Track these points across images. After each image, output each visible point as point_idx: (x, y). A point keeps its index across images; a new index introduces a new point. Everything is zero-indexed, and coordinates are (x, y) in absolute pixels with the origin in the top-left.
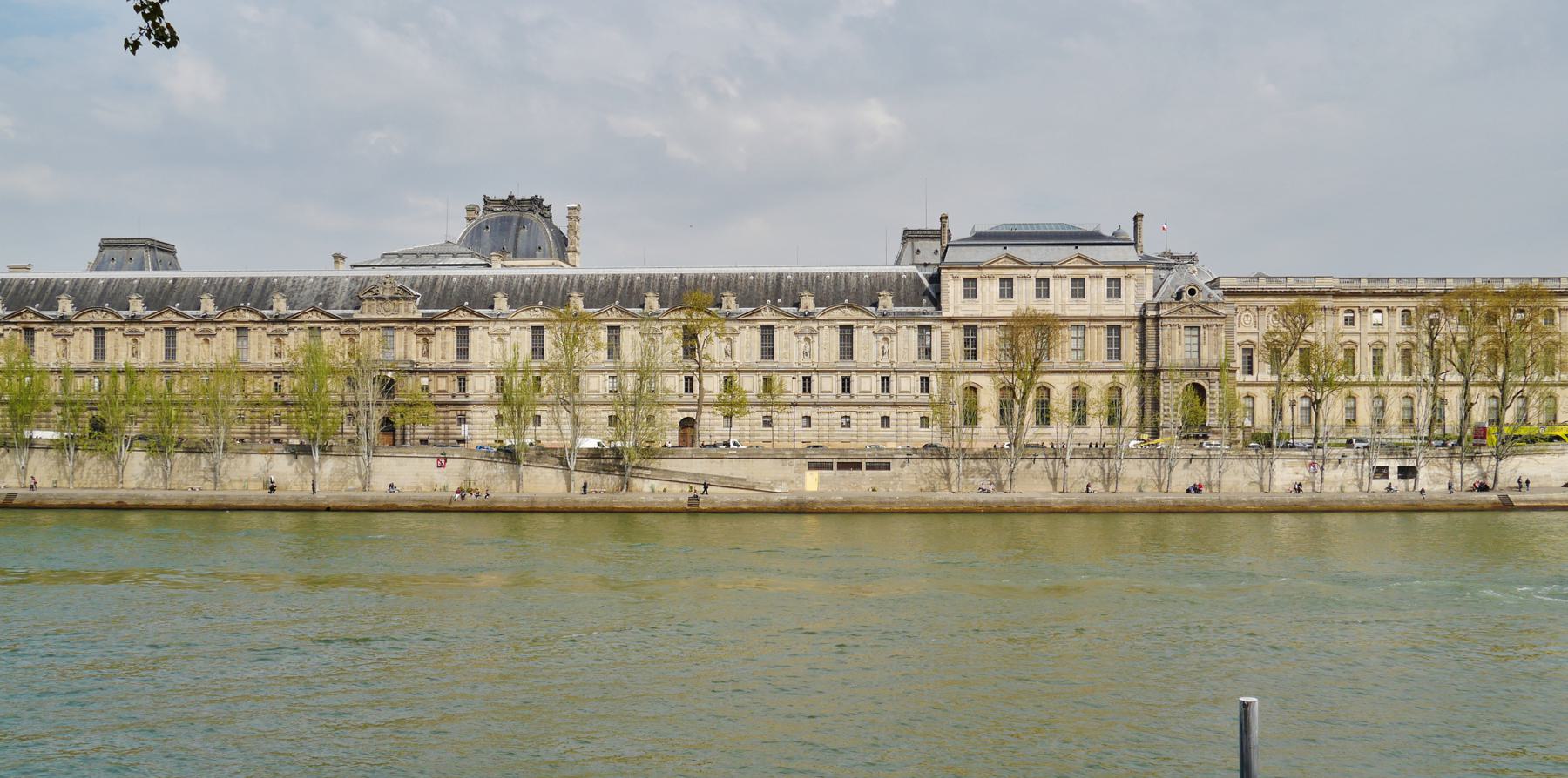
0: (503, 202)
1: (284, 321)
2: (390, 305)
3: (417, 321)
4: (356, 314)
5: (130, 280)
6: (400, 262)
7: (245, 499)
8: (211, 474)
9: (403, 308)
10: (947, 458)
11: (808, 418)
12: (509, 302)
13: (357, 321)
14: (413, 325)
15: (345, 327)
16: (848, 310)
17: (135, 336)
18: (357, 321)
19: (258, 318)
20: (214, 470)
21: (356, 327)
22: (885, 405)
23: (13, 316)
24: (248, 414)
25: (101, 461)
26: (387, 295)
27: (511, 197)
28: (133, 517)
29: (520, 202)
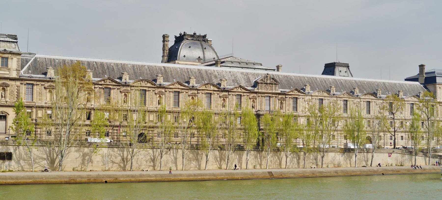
0: (191, 36)
1: (228, 91)
2: (268, 87)
3: (279, 94)
4: (256, 90)
5: (143, 66)
8: (315, 161)
9: (274, 88)
11: (402, 137)
13: (256, 93)
14: (277, 96)
15: (252, 95)
16: (413, 98)
17: (160, 95)
18: (256, 93)
19: (216, 89)
20: (315, 160)
21: (255, 95)
22: (402, 132)
23: (101, 81)
24: (111, 131)
25: (272, 156)
26: (269, 82)
27: (195, 34)
28: (210, 184)
29: (199, 36)
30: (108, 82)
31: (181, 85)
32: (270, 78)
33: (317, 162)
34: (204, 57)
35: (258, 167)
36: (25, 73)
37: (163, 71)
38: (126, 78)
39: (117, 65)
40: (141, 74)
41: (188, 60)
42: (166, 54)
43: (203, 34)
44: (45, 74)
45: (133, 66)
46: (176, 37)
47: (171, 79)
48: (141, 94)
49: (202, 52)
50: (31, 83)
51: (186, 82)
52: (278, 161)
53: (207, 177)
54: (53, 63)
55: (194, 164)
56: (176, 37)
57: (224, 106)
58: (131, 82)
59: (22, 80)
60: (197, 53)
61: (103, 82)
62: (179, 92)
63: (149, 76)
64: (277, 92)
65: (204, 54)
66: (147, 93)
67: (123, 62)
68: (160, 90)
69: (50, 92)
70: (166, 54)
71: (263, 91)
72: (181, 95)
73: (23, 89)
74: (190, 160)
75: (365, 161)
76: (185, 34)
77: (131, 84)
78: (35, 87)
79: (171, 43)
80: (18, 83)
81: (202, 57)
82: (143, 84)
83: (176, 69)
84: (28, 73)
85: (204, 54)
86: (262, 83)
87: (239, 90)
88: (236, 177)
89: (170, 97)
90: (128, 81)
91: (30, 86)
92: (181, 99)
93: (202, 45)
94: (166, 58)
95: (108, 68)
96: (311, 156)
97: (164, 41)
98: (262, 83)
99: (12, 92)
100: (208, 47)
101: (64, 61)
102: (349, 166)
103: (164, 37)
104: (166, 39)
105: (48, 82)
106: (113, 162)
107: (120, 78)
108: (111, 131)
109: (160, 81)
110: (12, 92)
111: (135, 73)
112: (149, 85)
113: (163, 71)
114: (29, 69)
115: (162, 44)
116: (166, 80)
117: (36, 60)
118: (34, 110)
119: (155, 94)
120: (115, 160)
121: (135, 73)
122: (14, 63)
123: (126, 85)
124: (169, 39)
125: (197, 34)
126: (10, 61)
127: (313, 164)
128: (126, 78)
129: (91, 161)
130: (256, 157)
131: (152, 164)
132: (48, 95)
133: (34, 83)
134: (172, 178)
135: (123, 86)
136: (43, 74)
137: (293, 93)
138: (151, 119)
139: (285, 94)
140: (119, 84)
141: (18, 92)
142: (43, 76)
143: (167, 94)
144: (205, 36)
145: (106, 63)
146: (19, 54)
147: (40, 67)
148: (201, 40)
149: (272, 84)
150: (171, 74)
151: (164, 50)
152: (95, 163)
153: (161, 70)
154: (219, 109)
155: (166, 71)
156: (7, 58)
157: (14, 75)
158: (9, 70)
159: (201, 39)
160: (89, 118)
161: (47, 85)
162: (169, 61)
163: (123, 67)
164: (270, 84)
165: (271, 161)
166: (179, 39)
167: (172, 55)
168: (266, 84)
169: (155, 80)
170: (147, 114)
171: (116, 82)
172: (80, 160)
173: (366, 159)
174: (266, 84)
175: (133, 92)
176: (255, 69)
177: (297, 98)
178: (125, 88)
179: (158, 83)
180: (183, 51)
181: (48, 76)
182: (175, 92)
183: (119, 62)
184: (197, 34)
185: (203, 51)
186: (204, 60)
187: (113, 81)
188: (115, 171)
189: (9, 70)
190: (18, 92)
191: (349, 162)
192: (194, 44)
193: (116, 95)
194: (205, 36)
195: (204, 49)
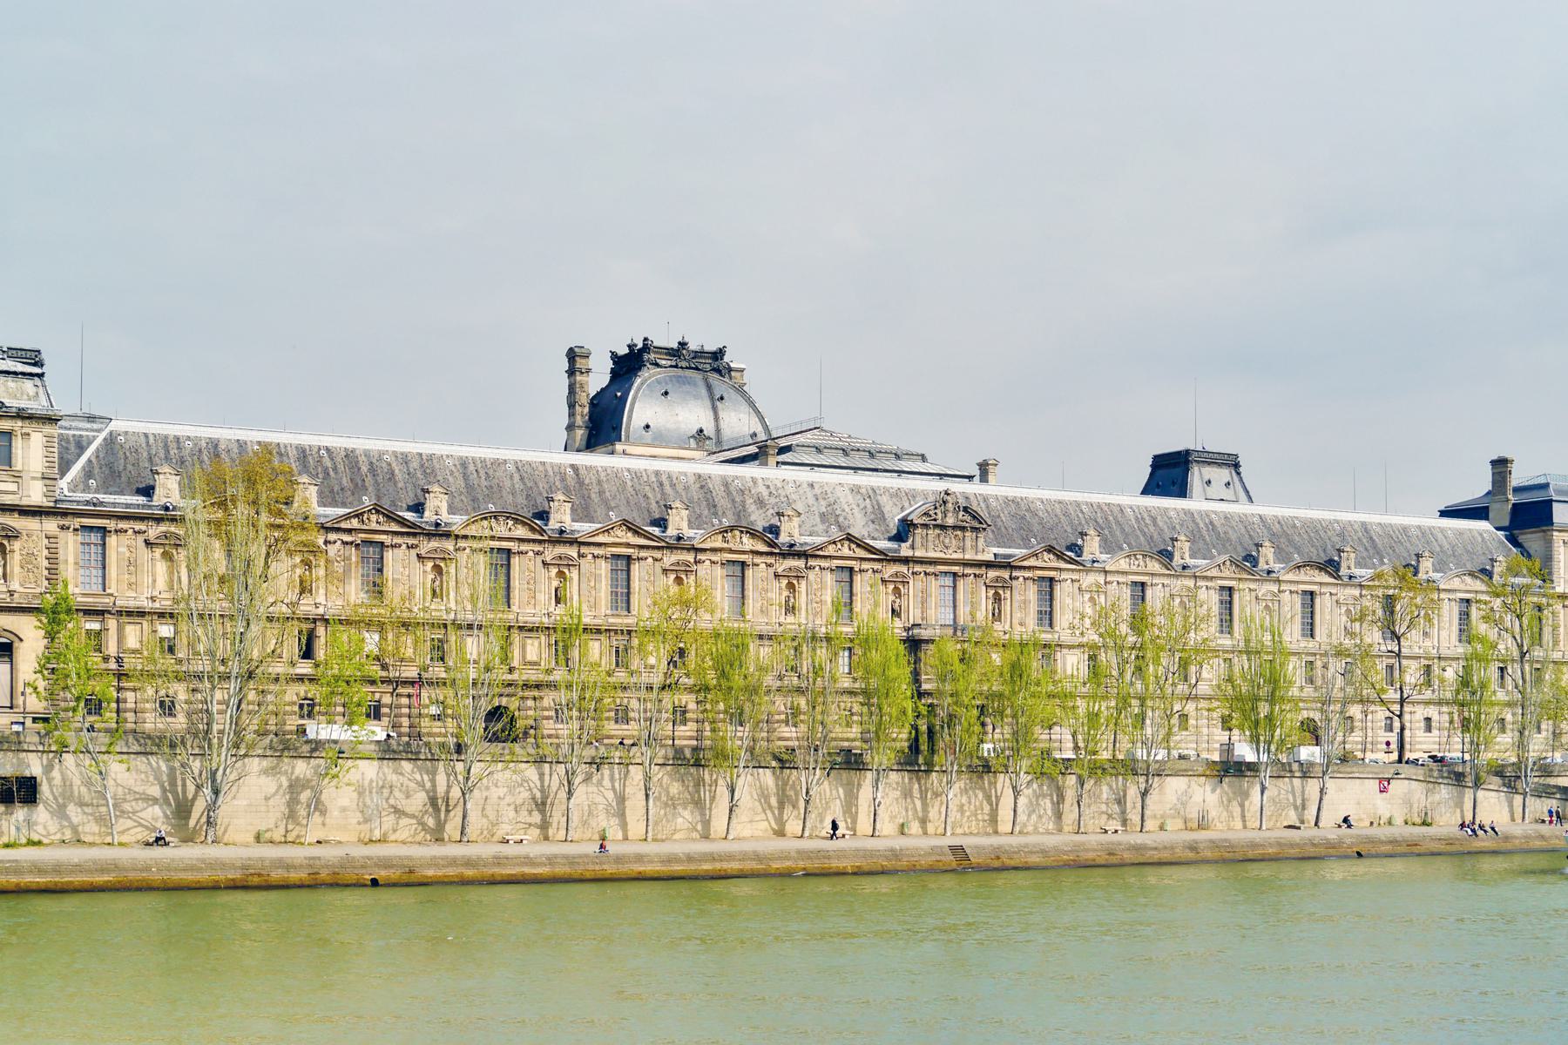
0: (672, 353)
1: (803, 555)
2: (950, 539)
3: (989, 565)
4: (905, 550)
5: (498, 463)
6: (842, 461)
7: (1254, 845)
8: (1116, 808)
9: (968, 543)
11: (1428, 720)
12: (320, 494)
13: (906, 561)
14: (982, 571)
15: (890, 570)
16: (1468, 579)
17: (562, 567)
18: (906, 561)
19: (763, 548)
20: (1119, 802)
21: (903, 569)
22: (1428, 703)
23: (347, 517)
25: (965, 791)
26: (950, 521)
27: (683, 344)
28: (743, 888)
29: (699, 354)
30: (374, 522)
31: (637, 532)
32: (957, 508)
33: (1123, 812)
34: (718, 431)
35: (915, 828)
36: (74, 487)
37: (571, 482)
38: (438, 507)
39: (405, 459)
40: (494, 491)
41: (661, 440)
42: (579, 421)
43: (711, 347)
44: (148, 491)
45: (464, 463)
46: (614, 356)
47: (600, 512)
48: (494, 566)
49: (710, 414)
50: (96, 525)
52: (987, 808)
53: (734, 866)
54: (173, 452)
56: (614, 356)
57: (790, 609)
58: (456, 522)
59: (64, 514)
60: (692, 414)
61: (355, 523)
63: (521, 500)
64: (980, 557)
65: (716, 419)
66: (515, 561)
67: (426, 448)
69: (167, 556)
70: (579, 421)
71: (932, 554)
72: (635, 567)
73: (70, 545)
74: (671, 804)
75: (1296, 808)
76: (646, 347)
77: (456, 529)
78: (112, 540)
79: (598, 378)
80: (51, 525)
81: (709, 430)
82: (501, 529)
83: (617, 474)
84: (87, 489)
85: (716, 419)
86: (925, 526)
87: (846, 551)
88: (835, 864)
89: (597, 578)
90: (445, 517)
91: (94, 538)
93: (709, 387)
94: (580, 434)
95: (373, 470)
96: (1105, 788)
97: (571, 372)
98: (925, 526)
99: (30, 556)
100: (730, 394)
101: (214, 444)
102: (1238, 824)
103: (572, 355)
104: (580, 363)
105: (159, 520)
106: (398, 812)
107: (418, 508)
108: (387, 699)
109: (562, 517)
110: (30, 556)
111: (470, 488)
112: (521, 532)
113: (571, 482)
114: (88, 473)
115: (565, 381)
116: (583, 512)
117: (111, 440)
118: (112, 623)
119: (545, 564)
120: (403, 804)
121: (470, 488)
122: (32, 451)
123: (439, 532)
124: (592, 363)
125: (693, 346)
126: (18, 443)
127: (1110, 817)
128: (438, 507)
129: (318, 806)
130: (907, 794)
132: (161, 567)
133: (111, 524)
134: (610, 869)
136: (140, 492)
137: (1039, 563)
138: (532, 655)
139: (1009, 566)
140: (414, 531)
141: (53, 559)
142: (141, 500)
144: (718, 355)
145: (367, 453)
146: (51, 420)
147: (127, 468)
149: (963, 529)
150: (601, 493)
151: (572, 406)
152: (334, 813)
155: (581, 483)
156: (9, 434)
157: (35, 495)
158: (17, 477)
159: (706, 364)
160: (308, 653)
161: (154, 531)
162: (591, 444)
163: (428, 467)
164: (954, 528)
165: (961, 808)
166: (628, 365)
167: (602, 424)
168: (943, 527)
169: (543, 515)
170: (516, 637)
171: (402, 522)
172: (280, 803)
173: (1299, 802)
174: (943, 527)
175: (463, 557)
176: (900, 472)
177: (1051, 580)
178: (434, 544)
179: (553, 524)
181: (159, 498)
182: (616, 557)
184: (693, 346)
185: (715, 409)
186: (719, 442)
187: (391, 517)
188: (405, 845)
189: (17, 477)
190: (53, 559)
191: (1237, 810)
192: (681, 381)
193: (405, 570)
195: (715, 400)
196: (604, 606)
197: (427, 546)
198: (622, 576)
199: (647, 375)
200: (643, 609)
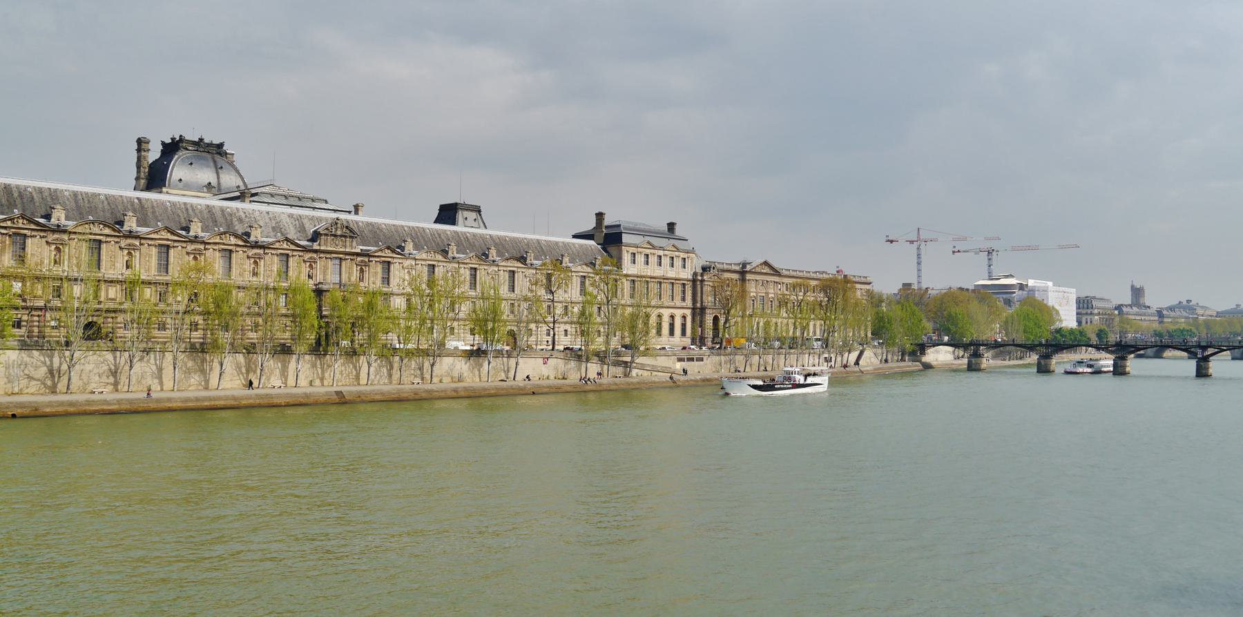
0: (194, 143)
1: (263, 247)
2: (339, 241)
3: (358, 254)
4: (316, 246)
10: (203, 351)
13: (316, 251)
15: (308, 256)
17: (131, 250)
18: (316, 251)
19: (241, 243)
23: (5, 220)
24: (25, 318)
25: (343, 364)
26: (339, 233)
27: (201, 140)
30: (21, 223)
31: (173, 233)
34: (219, 184)
35: (317, 382)
37: (137, 207)
39: (40, 191)
40: (92, 210)
41: (188, 187)
42: (142, 175)
43: (216, 142)
45: (75, 194)
46: (163, 144)
47: (153, 223)
51: (183, 229)
53: (222, 403)
55: (195, 379)
56: (163, 144)
57: (255, 274)
58: (70, 224)
60: (205, 175)
61: (9, 223)
62: (168, 247)
63: (108, 215)
66: (104, 246)
67: (53, 186)
68: (129, 241)
70: (142, 175)
72: (172, 251)
74: (188, 372)
77: (69, 228)
79: (154, 154)
81: (214, 183)
82: (96, 229)
83: (163, 203)
87: (285, 246)
88: (276, 401)
89: (150, 256)
90: (63, 222)
92: (171, 259)
93: (215, 162)
94: (143, 182)
97: (139, 150)
103: (139, 141)
104: (144, 145)
106: (30, 378)
107: (48, 217)
108: (25, 318)
109: (131, 224)
111: (78, 207)
112: (107, 231)
113: (137, 207)
115: (135, 154)
116: (142, 222)
119: (121, 248)
121: (78, 207)
123: (59, 229)
124: (150, 146)
130: (314, 366)
131: (112, 380)
134: (153, 406)
135: (54, 231)
138: (112, 294)
139: (369, 256)
140: (44, 229)
143: (144, 249)
144: (221, 145)
145: (18, 187)
148: (213, 152)
150: (153, 212)
151: (139, 167)
153: (133, 204)
154: (248, 279)
155: (142, 207)
159: (214, 150)
162: (148, 188)
163: (54, 196)
165: (341, 373)
166: (170, 149)
167: (155, 177)
168: (335, 236)
169: (121, 223)
170: (103, 286)
171: (38, 224)
174: (335, 236)
175: (73, 243)
178: (56, 236)
179: (126, 228)
180: (178, 171)
183: (45, 185)
184: (207, 141)
186: (219, 189)
187: (31, 221)
192: (200, 158)
193: (38, 250)
194: (221, 145)
195: (218, 169)
196: (154, 271)
197: (52, 237)
198: (164, 255)
199: (181, 154)
200: (175, 272)
